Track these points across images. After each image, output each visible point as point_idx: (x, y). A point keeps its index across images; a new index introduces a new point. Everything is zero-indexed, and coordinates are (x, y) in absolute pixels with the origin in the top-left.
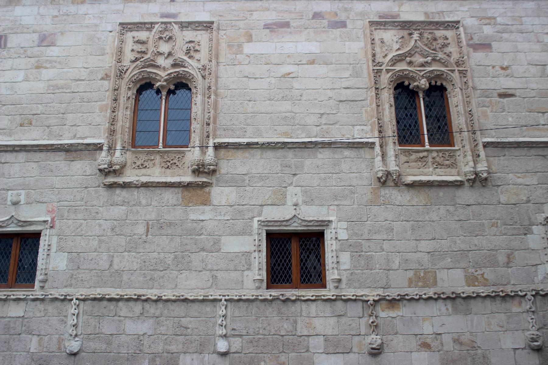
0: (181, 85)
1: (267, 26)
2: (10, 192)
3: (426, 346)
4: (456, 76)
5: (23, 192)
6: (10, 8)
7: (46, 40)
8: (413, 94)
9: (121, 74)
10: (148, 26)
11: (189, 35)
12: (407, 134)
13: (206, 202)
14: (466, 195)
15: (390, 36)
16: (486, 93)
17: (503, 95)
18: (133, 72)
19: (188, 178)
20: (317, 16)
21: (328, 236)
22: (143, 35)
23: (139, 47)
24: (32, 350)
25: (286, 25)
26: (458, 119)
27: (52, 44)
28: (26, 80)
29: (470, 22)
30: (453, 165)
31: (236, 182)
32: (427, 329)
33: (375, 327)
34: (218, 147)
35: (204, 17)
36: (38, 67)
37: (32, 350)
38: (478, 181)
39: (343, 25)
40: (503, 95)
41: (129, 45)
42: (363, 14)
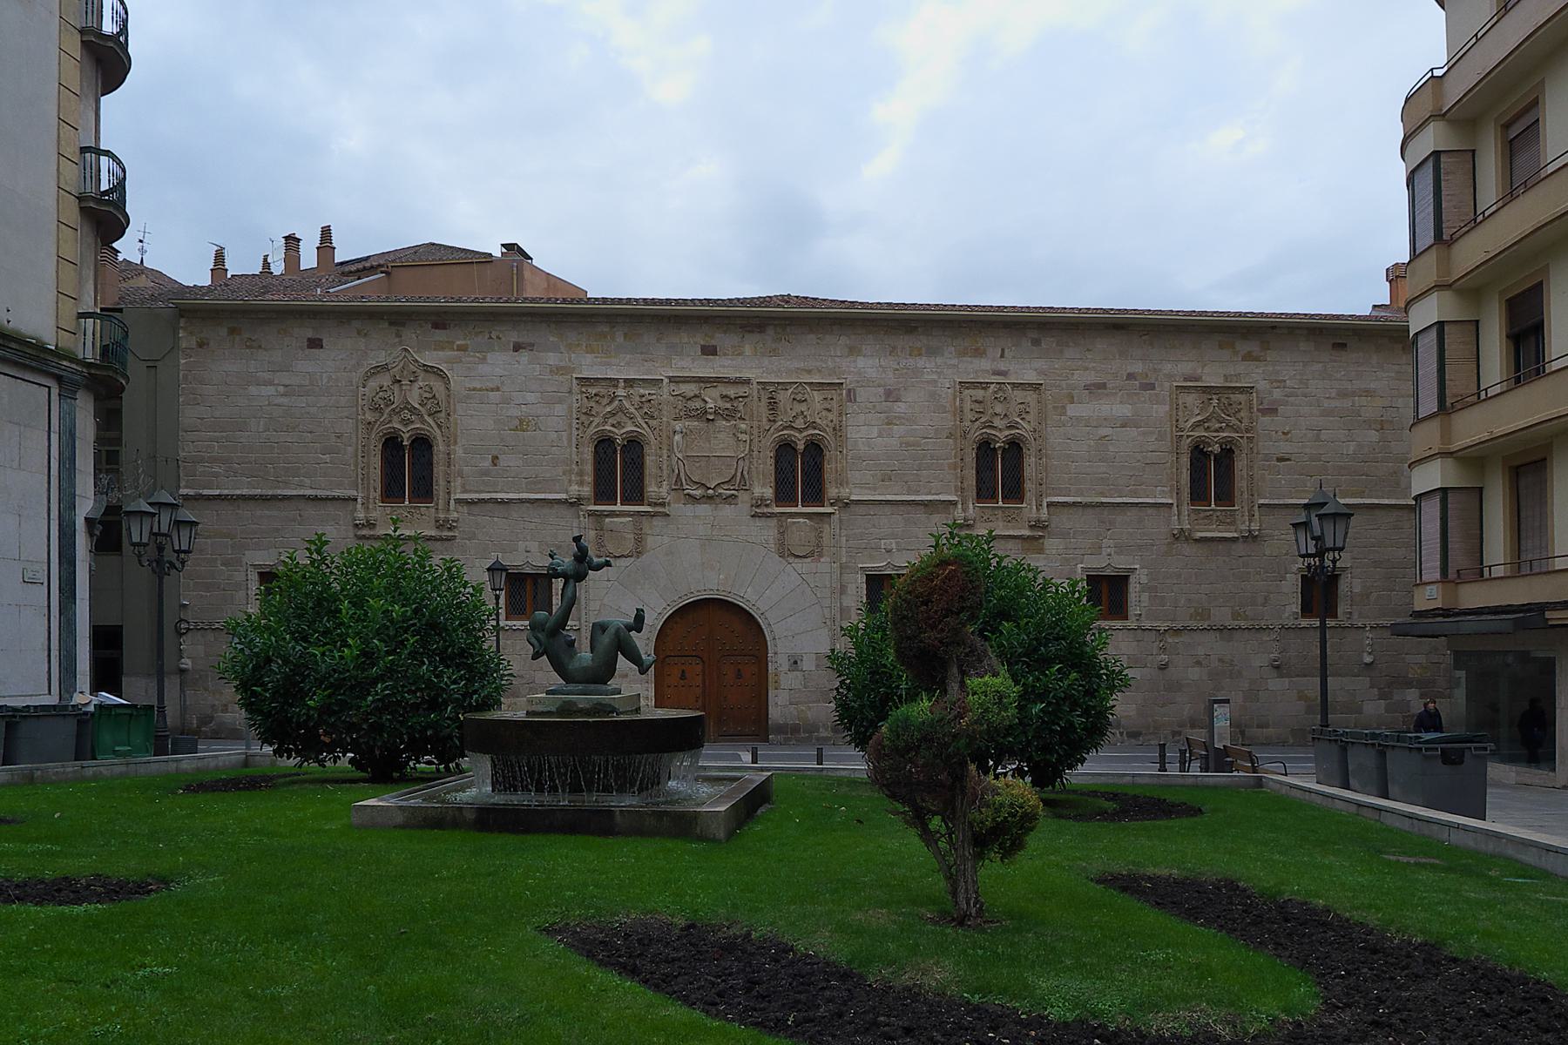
0: (1015, 448)
1: (1087, 387)
3: (1199, 663)
4: (1244, 442)
6: (851, 358)
7: (891, 395)
8: (1206, 455)
9: (965, 434)
10: (984, 386)
11: (1019, 395)
12: (1198, 494)
13: (1041, 551)
14: (1239, 548)
15: (1191, 399)
16: (1267, 458)
17: (1280, 460)
18: (976, 434)
19: (1027, 532)
20: (1131, 376)
21: (1132, 580)
22: (979, 394)
23: (977, 407)
25: (1104, 386)
26: (1241, 484)
29: (1262, 385)
30: (1233, 523)
31: (1064, 535)
32: (1201, 651)
33: (1163, 649)
34: (1050, 505)
35: (1030, 377)
38: (1251, 538)
39: (1152, 386)
40: (1280, 460)
41: (968, 405)
42: (1170, 377)
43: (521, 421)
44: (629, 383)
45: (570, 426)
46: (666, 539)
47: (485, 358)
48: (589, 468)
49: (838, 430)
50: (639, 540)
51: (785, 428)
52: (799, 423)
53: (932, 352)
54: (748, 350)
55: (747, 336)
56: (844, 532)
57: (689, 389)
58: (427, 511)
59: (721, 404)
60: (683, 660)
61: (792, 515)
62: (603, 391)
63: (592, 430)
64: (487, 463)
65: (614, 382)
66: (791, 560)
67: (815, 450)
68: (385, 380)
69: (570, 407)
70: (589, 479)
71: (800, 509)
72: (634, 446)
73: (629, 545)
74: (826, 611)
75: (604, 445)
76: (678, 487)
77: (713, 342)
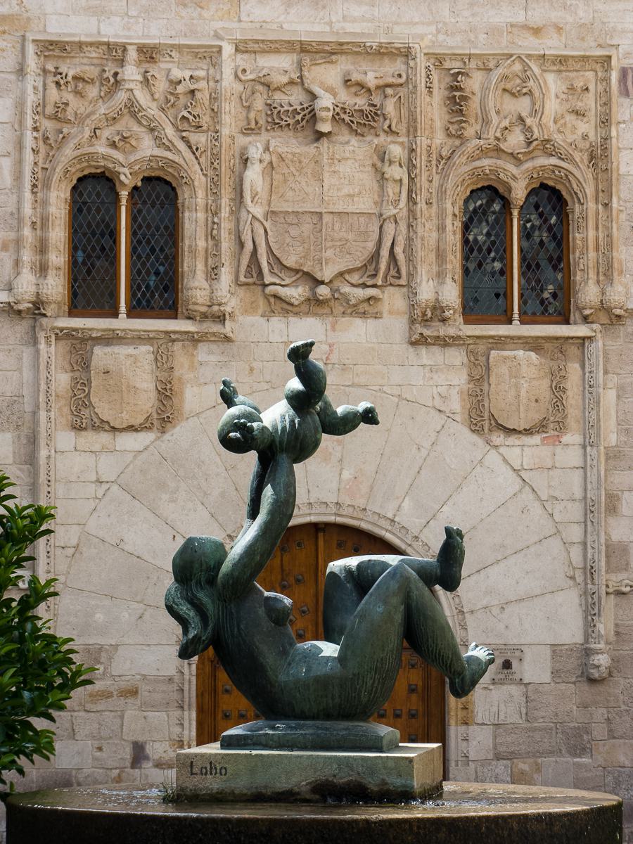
44: (149, 54)
45: (20, 145)
48: (59, 234)
49: (600, 156)
50: (167, 393)
51: (484, 152)
52: (515, 140)
56: (613, 380)
59: (345, 97)
61: (499, 342)
62: (92, 72)
63: (69, 152)
65: (116, 52)
66: (498, 438)
67: (551, 200)
69: (20, 105)
70: (58, 258)
71: (516, 329)
73: (146, 402)
74: (576, 555)
75: (93, 189)
76: (253, 277)
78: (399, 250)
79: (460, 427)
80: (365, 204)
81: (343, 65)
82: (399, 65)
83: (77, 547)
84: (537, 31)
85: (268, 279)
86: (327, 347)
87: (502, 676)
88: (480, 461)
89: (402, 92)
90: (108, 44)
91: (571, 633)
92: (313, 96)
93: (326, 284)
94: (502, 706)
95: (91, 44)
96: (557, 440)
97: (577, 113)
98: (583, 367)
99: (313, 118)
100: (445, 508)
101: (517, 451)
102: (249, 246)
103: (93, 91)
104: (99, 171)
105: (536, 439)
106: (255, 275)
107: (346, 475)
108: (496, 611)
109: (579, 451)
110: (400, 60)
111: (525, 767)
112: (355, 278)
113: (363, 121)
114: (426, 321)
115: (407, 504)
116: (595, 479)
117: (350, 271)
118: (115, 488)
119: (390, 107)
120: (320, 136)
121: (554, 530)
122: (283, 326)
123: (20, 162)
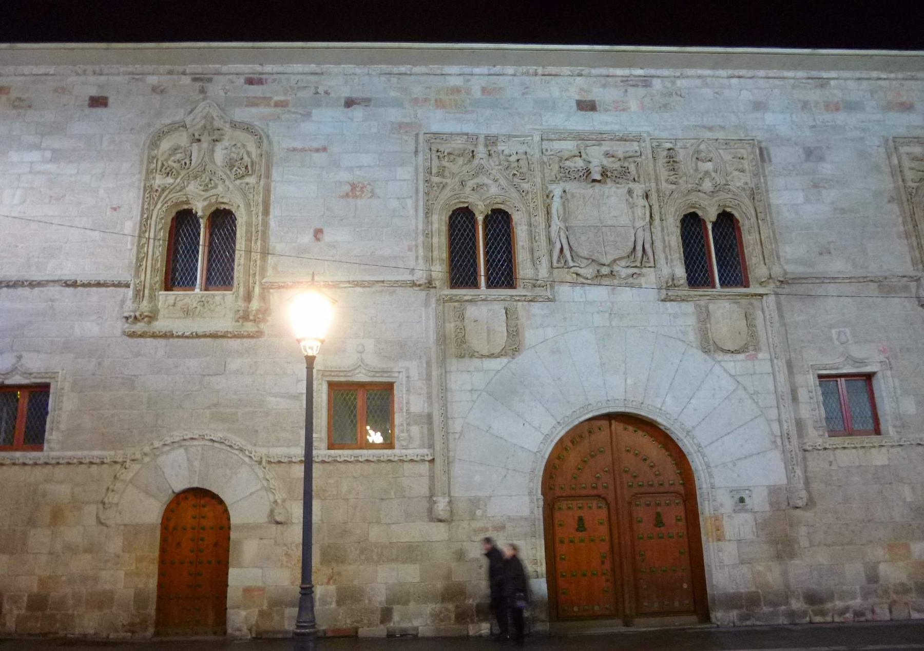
2: (833, 331)
5: (847, 330)
24: (908, 499)
27: (822, 159)
28: (807, 200)
36: (815, 186)
37: (908, 499)
43: (353, 186)
46: (550, 332)
47: (308, 115)
53: (851, 107)
54: (633, 105)
55: (631, 90)
57: (569, 146)
58: (225, 301)
60: (580, 503)
64: (307, 238)
65: (472, 138)
66: (720, 356)
68: (182, 139)
72: (500, 220)
73: (501, 338)
74: (775, 426)
75: (461, 219)
77: (590, 97)
78: (647, 246)
79: (695, 350)
80: (625, 220)
81: (606, 146)
82: (635, 146)
83: (461, 433)
84: (710, 129)
85: (571, 264)
86: (609, 304)
87: (739, 508)
88: (711, 370)
89: (639, 160)
90: (467, 134)
91: (778, 476)
92: (589, 162)
93: (608, 265)
94: (741, 528)
95: (458, 134)
96: (755, 357)
97: (742, 171)
98: (763, 313)
99: (588, 172)
100: (692, 401)
101: (732, 364)
102: (558, 246)
103: (461, 161)
104: (466, 205)
105: (741, 356)
106: (563, 262)
107: (629, 381)
108: (730, 465)
109: (769, 364)
110: (636, 144)
111: (760, 568)
112: (623, 263)
113: (622, 175)
114: (668, 288)
115: (669, 400)
116: (782, 380)
117: (620, 259)
118: (484, 393)
119: (632, 168)
120: (594, 181)
121: (760, 413)
122: (582, 292)
123: (417, 200)
